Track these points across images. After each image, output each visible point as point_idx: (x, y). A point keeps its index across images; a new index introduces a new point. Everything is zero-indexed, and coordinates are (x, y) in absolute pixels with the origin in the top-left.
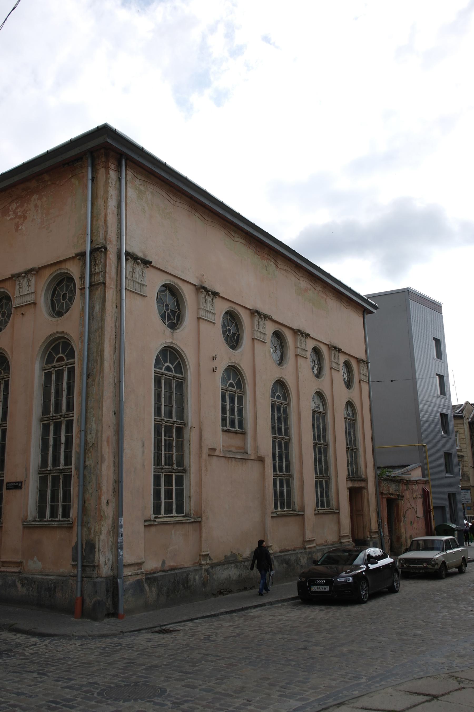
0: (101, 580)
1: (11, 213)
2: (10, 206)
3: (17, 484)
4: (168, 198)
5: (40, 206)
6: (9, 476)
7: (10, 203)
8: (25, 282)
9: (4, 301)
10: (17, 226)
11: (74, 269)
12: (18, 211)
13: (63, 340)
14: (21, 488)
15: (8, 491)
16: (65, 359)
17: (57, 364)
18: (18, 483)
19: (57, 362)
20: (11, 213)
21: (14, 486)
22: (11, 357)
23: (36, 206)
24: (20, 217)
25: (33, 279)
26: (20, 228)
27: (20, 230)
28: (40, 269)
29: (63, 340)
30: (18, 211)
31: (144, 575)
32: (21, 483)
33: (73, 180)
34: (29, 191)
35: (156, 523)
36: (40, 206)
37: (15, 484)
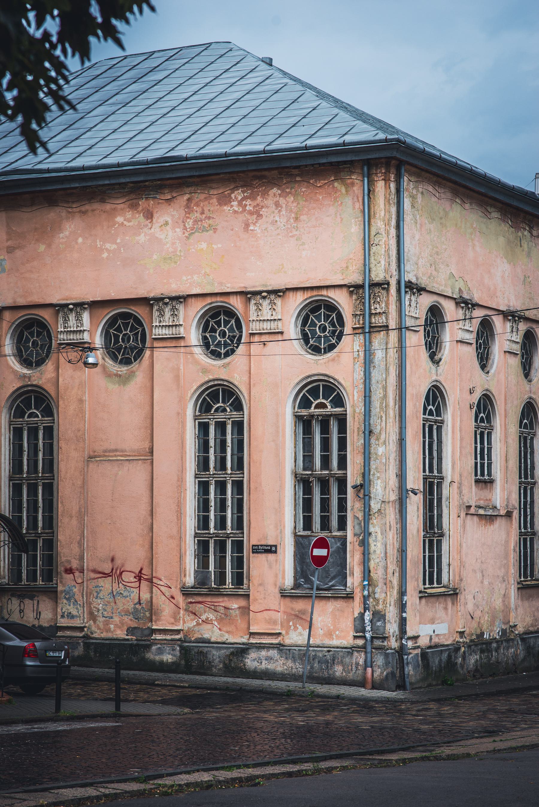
0: (393, 651)
1: (235, 203)
2: (232, 193)
3: (269, 548)
4: (434, 192)
5: (284, 206)
6: (254, 536)
7: (233, 190)
8: (265, 303)
9: (222, 317)
10: (247, 225)
11: (344, 302)
12: (248, 203)
13: (324, 383)
14: (275, 552)
15: (254, 555)
16: (329, 407)
17: (316, 410)
18: (271, 546)
19: (315, 408)
20: (235, 203)
21: (265, 550)
22: (246, 395)
23: (277, 205)
24: (251, 213)
25: (278, 302)
26: (251, 228)
27: (252, 230)
28: (287, 289)
29: (324, 383)
30: (248, 203)
31: (420, 650)
32: (276, 546)
33: (336, 184)
34: (264, 181)
35: (427, 595)
36: (284, 206)
37: (266, 548)
